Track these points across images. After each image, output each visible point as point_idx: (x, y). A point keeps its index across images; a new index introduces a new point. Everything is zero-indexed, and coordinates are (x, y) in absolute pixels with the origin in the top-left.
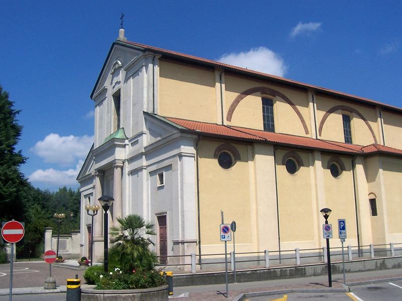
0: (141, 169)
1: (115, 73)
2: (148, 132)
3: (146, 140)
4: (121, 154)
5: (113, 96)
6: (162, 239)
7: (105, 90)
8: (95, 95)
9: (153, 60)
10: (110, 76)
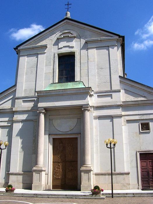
0: (120, 116)
1: (70, 39)
2: (122, 91)
3: (122, 97)
4: (92, 101)
5: (58, 54)
6: (143, 168)
7: (45, 47)
8: (21, 47)
9: (121, 45)
10: (54, 38)
